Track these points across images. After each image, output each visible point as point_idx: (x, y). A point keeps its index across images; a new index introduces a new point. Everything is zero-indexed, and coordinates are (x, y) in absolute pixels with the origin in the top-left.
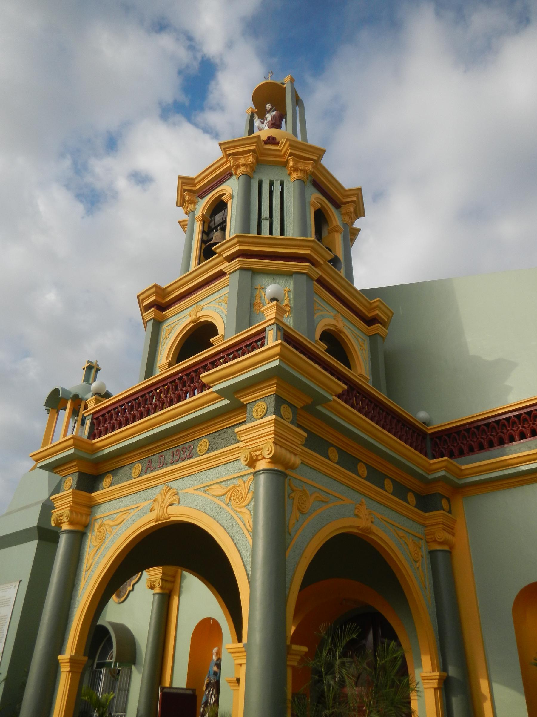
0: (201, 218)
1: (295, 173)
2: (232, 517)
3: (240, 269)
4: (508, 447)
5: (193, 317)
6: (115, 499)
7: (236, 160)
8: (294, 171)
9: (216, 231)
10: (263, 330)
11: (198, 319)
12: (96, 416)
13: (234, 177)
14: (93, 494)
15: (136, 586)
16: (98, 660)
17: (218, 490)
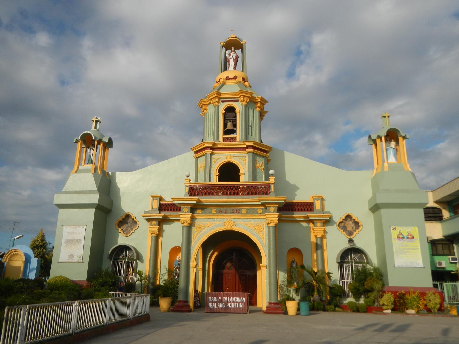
0: (223, 113)
1: (259, 108)
2: (256, 234)
3: (253, 153)
4: (295, 213)
5: (229, 160)
6: (204, 218)
7: (244, 98)
8: (259, 108)
9: (230, 122)
10: (270, 184)
11: (230, 161)
12: (190, 186)
13: (239, 102)
14: (194, 215)
15: (135, 231)
16: (114, 257)
17: (251, 225)
